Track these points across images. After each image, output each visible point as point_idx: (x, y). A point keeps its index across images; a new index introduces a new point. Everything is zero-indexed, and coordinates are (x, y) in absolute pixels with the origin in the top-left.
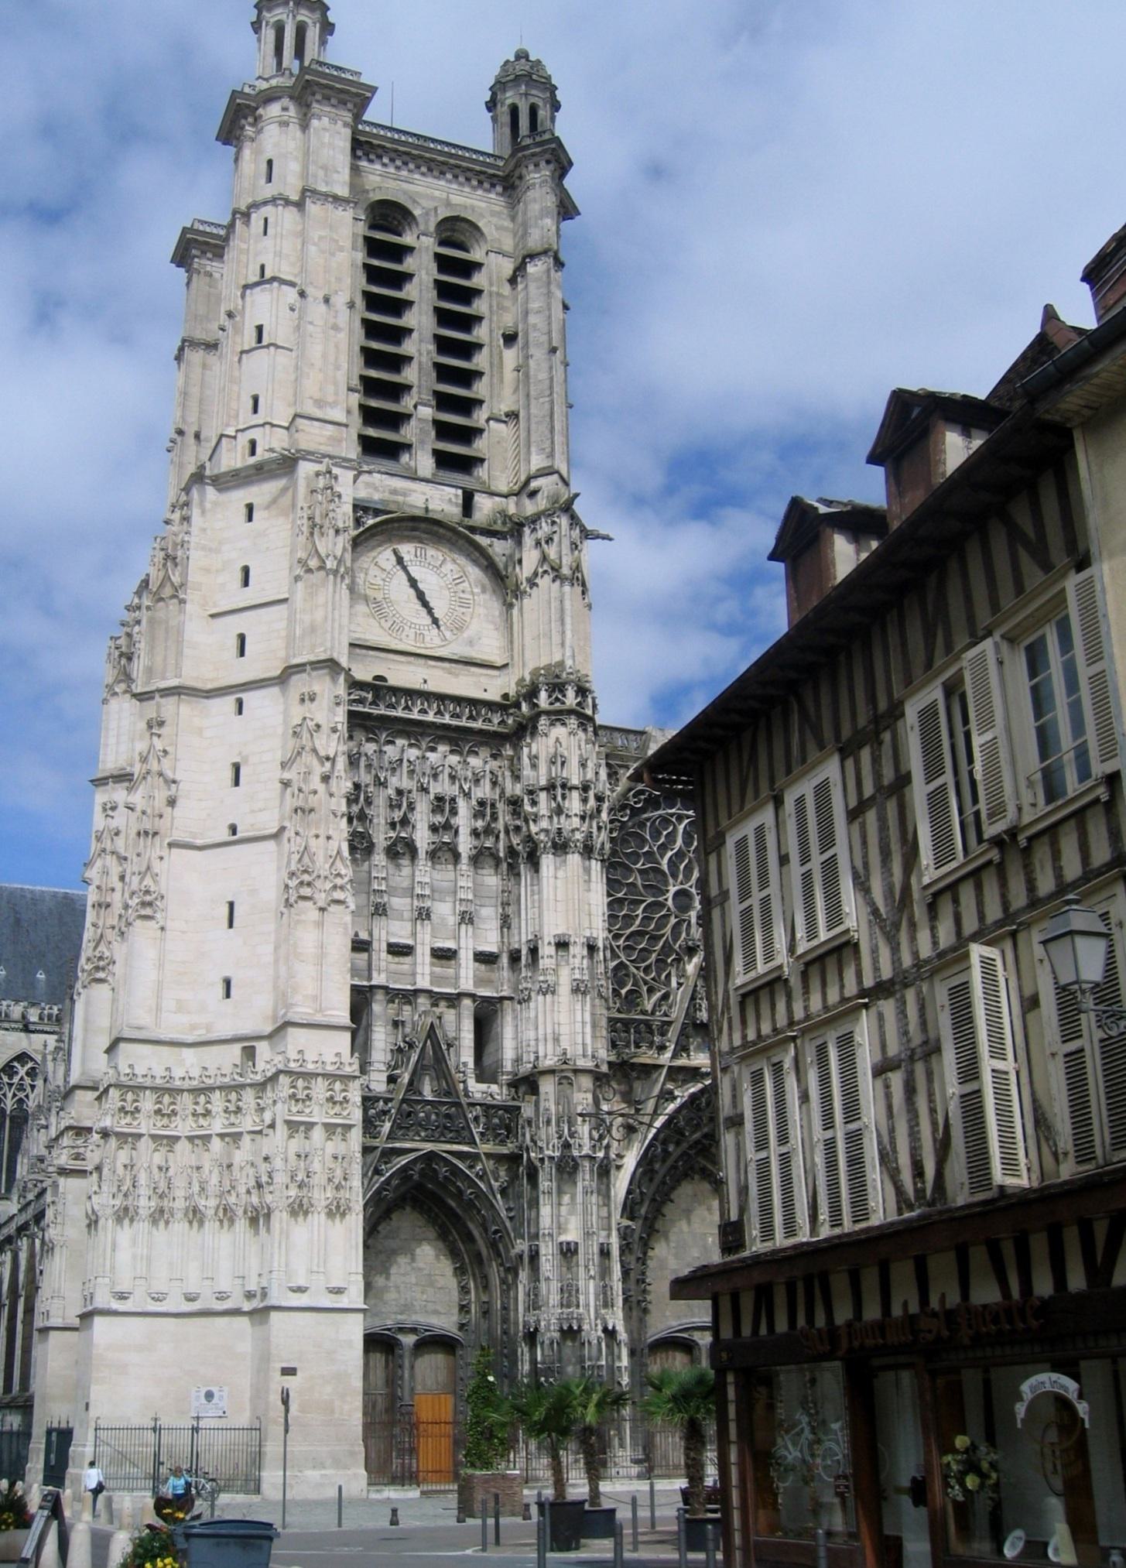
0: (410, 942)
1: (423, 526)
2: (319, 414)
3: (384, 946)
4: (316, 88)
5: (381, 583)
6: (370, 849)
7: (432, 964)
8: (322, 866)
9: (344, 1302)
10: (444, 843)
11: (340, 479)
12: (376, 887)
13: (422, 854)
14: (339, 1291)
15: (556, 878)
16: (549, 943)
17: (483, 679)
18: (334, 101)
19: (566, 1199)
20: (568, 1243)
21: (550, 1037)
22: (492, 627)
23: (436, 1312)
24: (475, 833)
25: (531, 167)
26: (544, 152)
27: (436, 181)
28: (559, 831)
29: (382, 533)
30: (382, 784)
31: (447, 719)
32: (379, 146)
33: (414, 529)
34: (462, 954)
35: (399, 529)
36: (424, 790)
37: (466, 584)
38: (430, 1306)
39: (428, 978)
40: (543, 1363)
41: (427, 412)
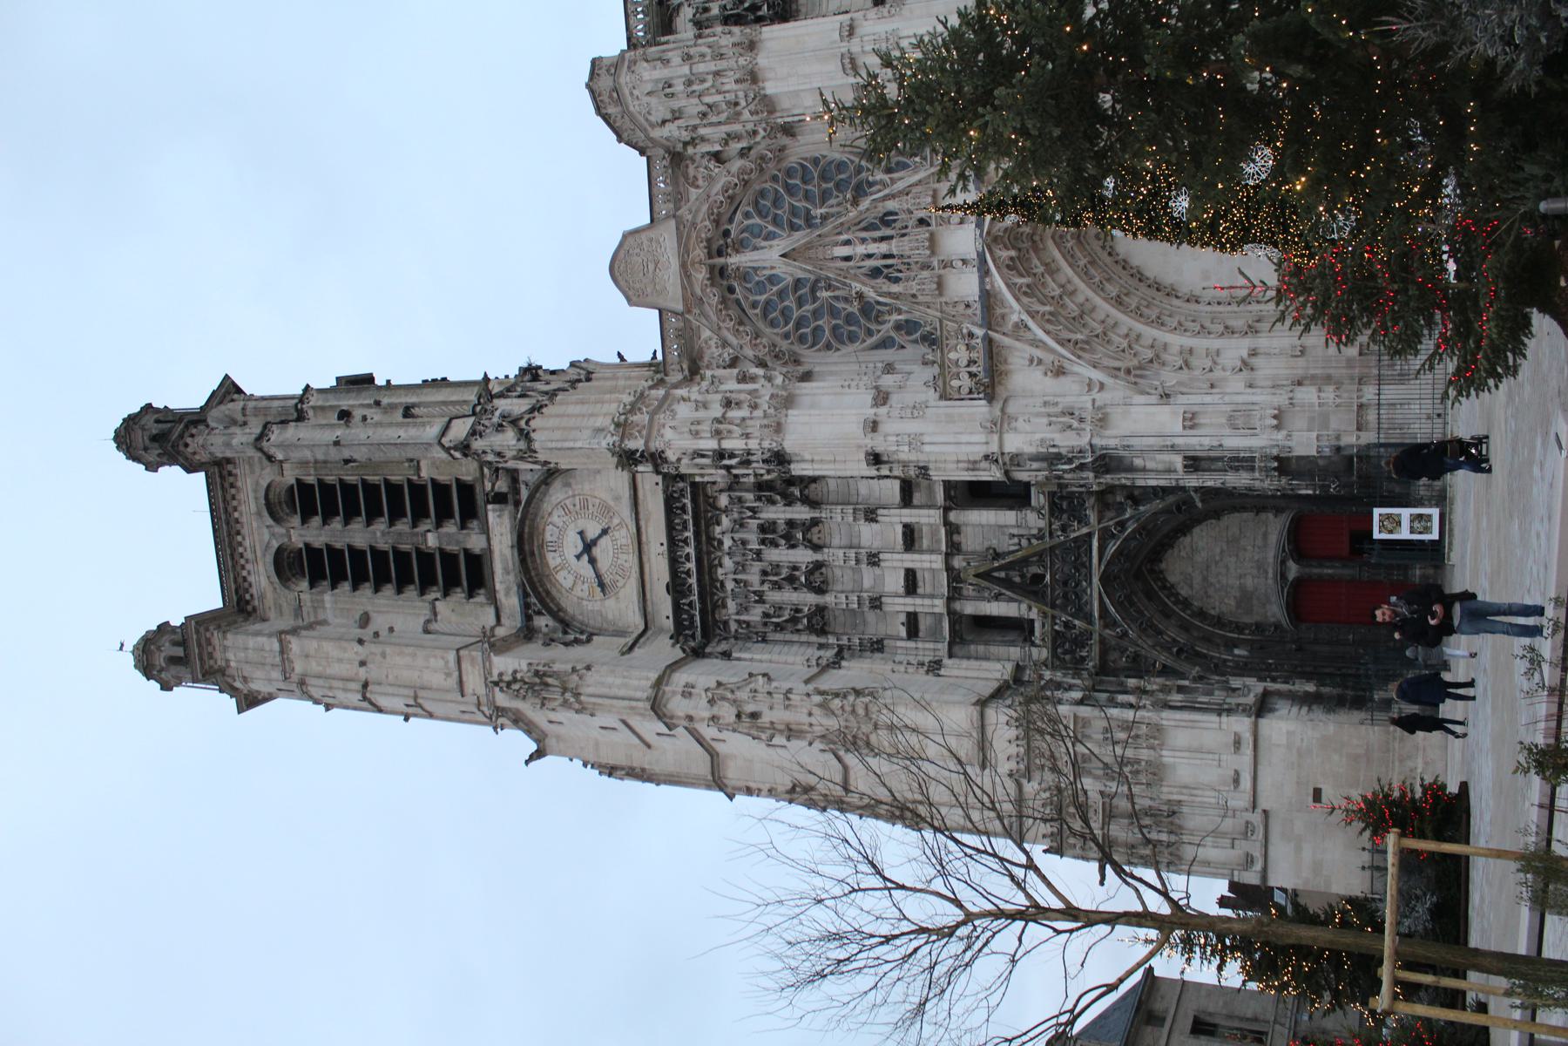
0: (902, 573)
1: (527, 548)
2: (456, 674)
3: (909, 600)
4: (207, 667)
5: (586, 585)
7: (921, 552)
8: (832, 723)
9: (1247, 737)
10: (804, 539)
11: (502, 669)
12: (856, 606)
13: (818, 557)
14: (1237, 743)
15: (813, 461)
16: (878, 470)
17: (647, 487)
19: (1138, 462)
20: (1185, 466)
21: (971, 473)
22: (598, 477)
23: (1265, 536)
24: (789, 504)
25: (197, 457)
26: (178, 453)
27: (245, 526)
28: (764, 461)
29: (543, 585)
30: (761, 601)
31: (689, 534)
32: (235, 582)
33: (533, 554)
34: (907, 520)
35: (536, 569)
36: (758, 553)
37: (567, 502)
38: (1259, 542)
39: (934, 557)
41: (432, 541)
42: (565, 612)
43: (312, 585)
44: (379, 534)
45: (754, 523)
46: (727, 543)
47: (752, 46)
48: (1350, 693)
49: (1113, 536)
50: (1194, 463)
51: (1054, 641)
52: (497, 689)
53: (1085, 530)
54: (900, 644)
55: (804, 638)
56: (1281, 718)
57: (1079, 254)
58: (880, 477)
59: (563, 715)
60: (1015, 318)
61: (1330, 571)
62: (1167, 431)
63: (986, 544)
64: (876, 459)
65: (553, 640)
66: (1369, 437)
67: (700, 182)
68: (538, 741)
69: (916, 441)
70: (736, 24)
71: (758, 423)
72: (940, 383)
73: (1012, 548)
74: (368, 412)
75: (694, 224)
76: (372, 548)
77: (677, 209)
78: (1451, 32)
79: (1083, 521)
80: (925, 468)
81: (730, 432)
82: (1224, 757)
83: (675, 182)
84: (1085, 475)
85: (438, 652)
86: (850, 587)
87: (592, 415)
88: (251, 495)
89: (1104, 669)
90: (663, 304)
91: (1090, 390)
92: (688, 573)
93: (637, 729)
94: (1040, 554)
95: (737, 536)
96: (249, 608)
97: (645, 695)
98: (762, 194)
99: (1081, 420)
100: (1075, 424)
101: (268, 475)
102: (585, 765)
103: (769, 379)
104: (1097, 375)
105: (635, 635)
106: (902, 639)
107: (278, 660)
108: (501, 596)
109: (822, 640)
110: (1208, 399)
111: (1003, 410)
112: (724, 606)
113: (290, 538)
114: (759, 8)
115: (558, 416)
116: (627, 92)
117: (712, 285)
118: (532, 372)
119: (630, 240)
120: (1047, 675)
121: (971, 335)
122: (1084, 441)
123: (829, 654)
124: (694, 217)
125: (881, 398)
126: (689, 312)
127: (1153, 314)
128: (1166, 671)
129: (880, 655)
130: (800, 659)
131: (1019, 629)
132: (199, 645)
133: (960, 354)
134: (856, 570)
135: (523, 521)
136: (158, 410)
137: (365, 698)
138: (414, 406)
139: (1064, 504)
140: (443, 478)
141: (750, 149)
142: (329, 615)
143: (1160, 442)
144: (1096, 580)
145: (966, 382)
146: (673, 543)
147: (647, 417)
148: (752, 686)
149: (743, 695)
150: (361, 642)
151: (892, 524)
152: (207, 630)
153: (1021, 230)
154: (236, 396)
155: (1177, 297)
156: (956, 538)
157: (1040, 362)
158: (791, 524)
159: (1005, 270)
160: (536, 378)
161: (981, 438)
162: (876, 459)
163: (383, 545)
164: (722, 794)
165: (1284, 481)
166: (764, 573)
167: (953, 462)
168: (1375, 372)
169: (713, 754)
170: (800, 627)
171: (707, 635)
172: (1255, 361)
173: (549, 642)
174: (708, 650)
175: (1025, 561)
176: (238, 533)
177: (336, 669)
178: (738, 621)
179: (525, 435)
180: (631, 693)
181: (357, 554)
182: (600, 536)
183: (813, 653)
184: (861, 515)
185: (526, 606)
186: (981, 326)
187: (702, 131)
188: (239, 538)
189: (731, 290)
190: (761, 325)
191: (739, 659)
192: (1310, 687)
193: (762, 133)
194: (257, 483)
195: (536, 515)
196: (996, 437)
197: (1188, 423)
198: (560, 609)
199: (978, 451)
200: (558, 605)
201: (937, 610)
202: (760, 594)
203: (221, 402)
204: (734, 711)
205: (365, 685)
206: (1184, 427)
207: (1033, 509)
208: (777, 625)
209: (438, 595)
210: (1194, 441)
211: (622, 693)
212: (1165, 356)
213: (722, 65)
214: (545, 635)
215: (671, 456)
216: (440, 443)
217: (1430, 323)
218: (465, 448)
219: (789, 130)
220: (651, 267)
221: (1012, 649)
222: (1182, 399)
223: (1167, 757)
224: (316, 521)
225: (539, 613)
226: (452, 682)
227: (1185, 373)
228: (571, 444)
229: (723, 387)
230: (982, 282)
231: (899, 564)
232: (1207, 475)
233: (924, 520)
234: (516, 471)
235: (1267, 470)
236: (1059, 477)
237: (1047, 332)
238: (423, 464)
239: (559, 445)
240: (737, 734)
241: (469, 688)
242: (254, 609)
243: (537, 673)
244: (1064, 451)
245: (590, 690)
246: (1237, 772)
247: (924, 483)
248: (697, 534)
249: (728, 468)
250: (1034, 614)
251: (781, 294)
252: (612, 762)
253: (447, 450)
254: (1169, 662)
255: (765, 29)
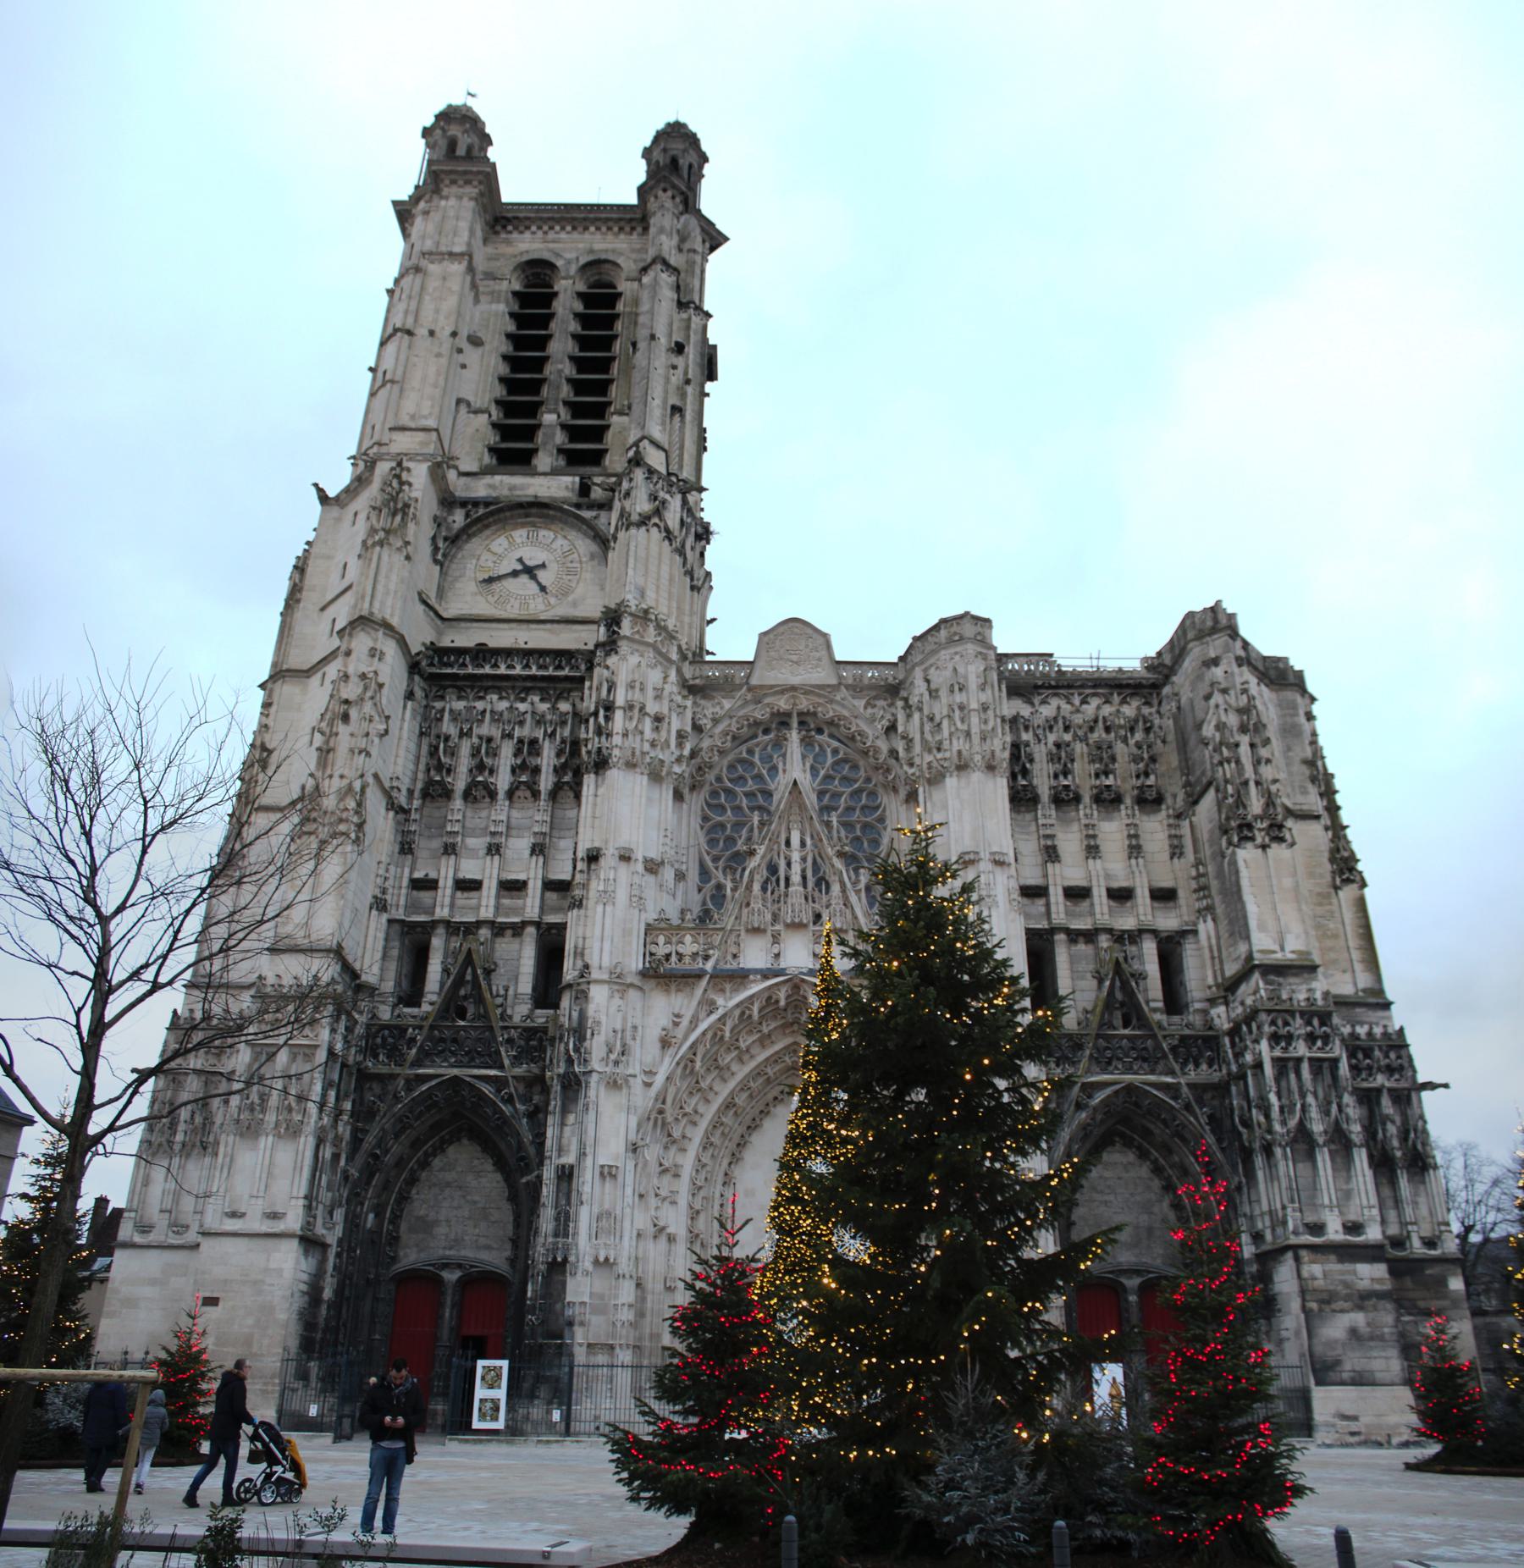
0: (478, 877)
1: (534, 511)
2: (413, 425)
3: (450, 883)
6: (447, 794)
7: (498, 897)
9: (279, 1227)
11: (414, 472)
13: (501, 795)
14: (274, 1216)
17: (584, 635)
18: (461, 182)
19: (571, 1118)
24: (556, 770)
26: (659, 181)
28: (600, 749)
29: (495, 522)
30: (462, 735)
31: (534, 671)
33: (527, 516)
34: (531, 884)
35: (512, 517)
36: (510, 736)
38: (482, 1241)
39: (491, 910)
41: (549, 418)
42: (467, 541)
43: (515, 294)
44: (560, 366)
45: (539, 734)
46: (522, 707)
47: (991, 768)
48: (319, 1336)
49: (499, 1091)
50: (566, 1175)
51: (396, 1027)
52: (394, 464)
53: (506, 1062)
54: (407, 871)
55: (421, 776)
56: (297, 1262)
57: (777, 1068)
58: (575, 861)
59: (361, 527)
60: (720, 1001)
61: (447, 1314)
62: (601, 1151)
63: (500, 963)
64: (593, 857)
65: (439, 525)
66: (580, 1356)
67: (870, 710)
68: (337, 498)
69: (607, 897)
70: (1012, 755)
71: (637, 745)
72: (663, 925)
73: (494, 988)
74: (680, 371)
75: (831, 701)
76: (547, 358)
77: (847, 687)
78: (961, 1431)
79: (516, 1061)
80: (580, 906)
81: (631, 718)
82: (260, 1202)
83: (871, 687)
84: (562, 1064)
85: (437, 410)
86: (468, 824)
87: (658, 587)
88: (610, 246)
89: (363, 1077)
90: (758, 666)
91: (646, 1073)
92: (495, 666)
93: (341, 600)
94: (486, 1016)
95: (528, 717)
96: (498, 228)
97: (375, 611)
98: (855, 767)
99: (616, 1063)
100: (613, 1057)
101: (628, 265)
102: (308, 543)
103: (679, 760)
104: (659, 1080)
105: (437, 607)
106: (411, 873)
107: (443, 249)
108: (488, 479)
109: (417, 794)
110: (629, 1191)
111: (631, 985)
112: (460, 698)
113: (565, 278)
114: (1024, 777)
115: (660, 554)
116: (958, 649)
117: (773, 714)
118: (704, 534)
119: (821, 640)
120: (362, 1019)
121: (707, 958)
122: (595, 1064)
123: (402, 800)
124: (838, 703)
125: (652, 867)
126: (750, 689)
127: (716, 1140)
128: (356, 1141)
129: (397, 849)
130: (399, 770)
131: (412, 995)
132: (465, 173)
133: (689, 946)
134: (485, 831)
135: (561, 510)
136: (701, 167)
137: (396, 330)
138: (682, 417)
139: (535, 1042)
140: (610, 436)
141: (897, 759)
142: (484, 306)
143: (590, 1141)
144: (456, 1072)
145: (661, 950)
146: (527, 654)
147: (651, 640)
148: (377, 718)
149: (368, 708)
150: (454, 334)
151: (528, 869)
152: (480, 182)
154: (707, 245)
156: (509, 932)
157: (676, 1024)
158: (536, 770)
159: (766, 995)
160: (698, 537)
161: (606, 962)
162: (593, 857)
163: (549, 370)
164: (265, 677)
165: (542, 1267)
166: (490, 740)
168: (646, 1363)
169: (308, 673)
170: (432, 773)
171: (432, 679)
172: (663, 1239)
173: (438, 522)
174: (417, 678)
175: (480, 1000)
176: (574, 228)
177: (428, 307)
178: (443, 710)
179: (644, 521)
180: (379, 595)
181: (542, 342)
182: (539, 584)
183: (404, 785)
184: (539, 840)
185: (476, 503)
186: (715, 968)
187: (917, 716)
188: (569, 228)
189: (766, 731)
190: (731, 757)
191: (405, 707)
192: (327, 1294)
193: (911, 771)
194: (621, 254)
195: (565, 523)
196: (605, 977)
197: (606, 1170)
198: (470, 537)
199: (593, 959)
200: (474, 535)
201: (438, 910)
202: (469, 734)
203: (703, 230)
204: (352, 697)
205: (409, 333)
207: (532, 1011)
208: (437, 748)
209: (494, 418)
210: (588, 1175)
211: (380, 587)
212: (673, 1149)
213: (976, 739)
214: (445, 519)
215: (612, 661)
216: (644, 438)
217: (686, 1413)
218: (637, 461)
219: (912, 798)
220: (794, 658)
221: (392, 984)
222: (630, 1165)
223: (265, 1142)
224: (579, 307)
225: (467, 515)
226: (405, 420)
227: (654, 1168)
228: (631, 565)
229: (674, 716)
230: (756, 971)
231: (487, 874)
232: (553, 1188)
233: (529, 901)
234: (610, 508)
235: (555, 1249)
236: (561, 1038)
237: (704, 1033)
238: (625, 419)
239: (632, 553)
240: (327, 698)
241: (397, 436)
242: (496, 233)
243: (407, 506)
244: (587, 1044)
245: (385, 557)
246: (243, 1215)
247: (566, 904)
248: (533, 678)
249: (596, 714)
250: (426, 1007)
251: (759, 777)
252: (309, 571)
253: (636, 444)
254: (365, 1146)
255: (1005, 781)
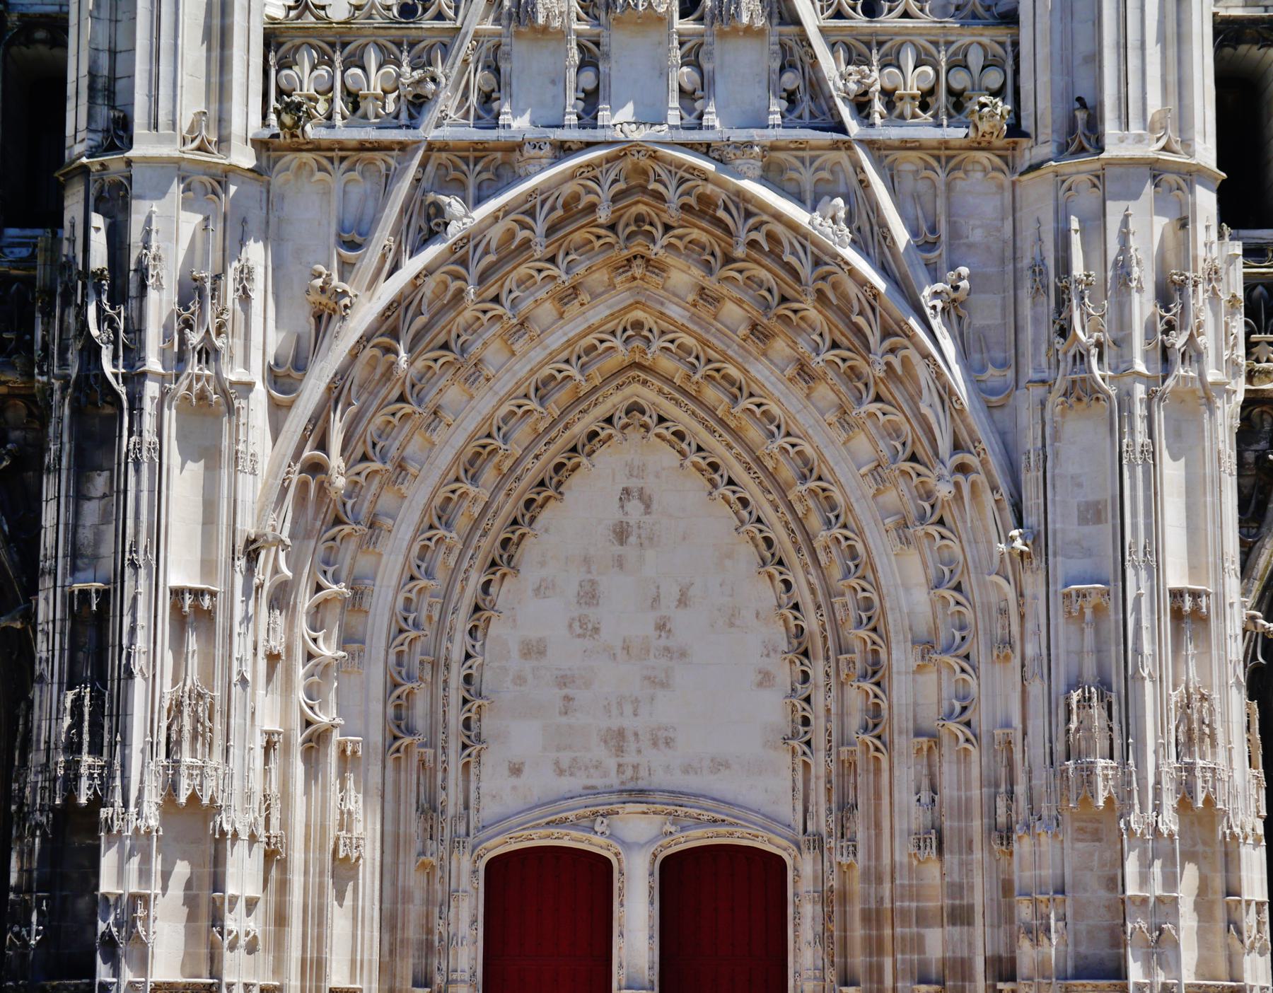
19: (99, 483)
20: (85, 594)
21: (84, 83)
40: (17, 889)
60: (454, 205)
153: (658, 233)
155: (487, 585)
167: (112, 40)
206: (177, 593)
